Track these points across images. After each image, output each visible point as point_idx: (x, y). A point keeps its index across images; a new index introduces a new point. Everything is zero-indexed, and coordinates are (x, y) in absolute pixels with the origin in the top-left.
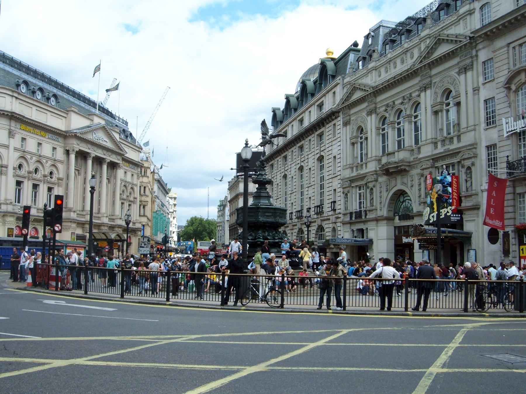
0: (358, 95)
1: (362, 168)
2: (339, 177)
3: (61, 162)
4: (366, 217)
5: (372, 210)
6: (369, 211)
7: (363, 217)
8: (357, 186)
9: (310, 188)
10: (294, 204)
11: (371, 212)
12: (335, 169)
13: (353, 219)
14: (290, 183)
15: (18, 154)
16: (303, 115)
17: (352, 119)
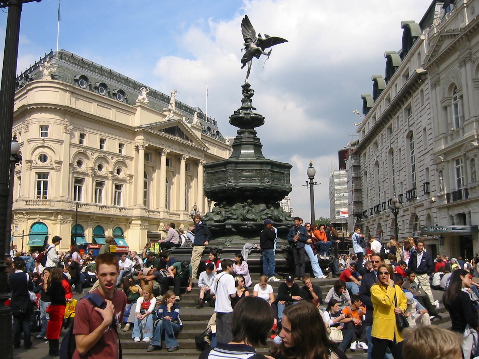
0: (447, 44)
1: (458, 135)
2: (431, 152)
3: (131, 158)
4: (467, 197)
5: (475, 187)
6: (471, 188)
7: (464, 198)
8: (453, 159)
9: (401, 172)
10: (387, 192)
11: (474, 191)
12: (426, 144)
13: (451, 201)
14: (382, 169)
15: (74, 150)
16: (390, 91)
17: (441, 78)
